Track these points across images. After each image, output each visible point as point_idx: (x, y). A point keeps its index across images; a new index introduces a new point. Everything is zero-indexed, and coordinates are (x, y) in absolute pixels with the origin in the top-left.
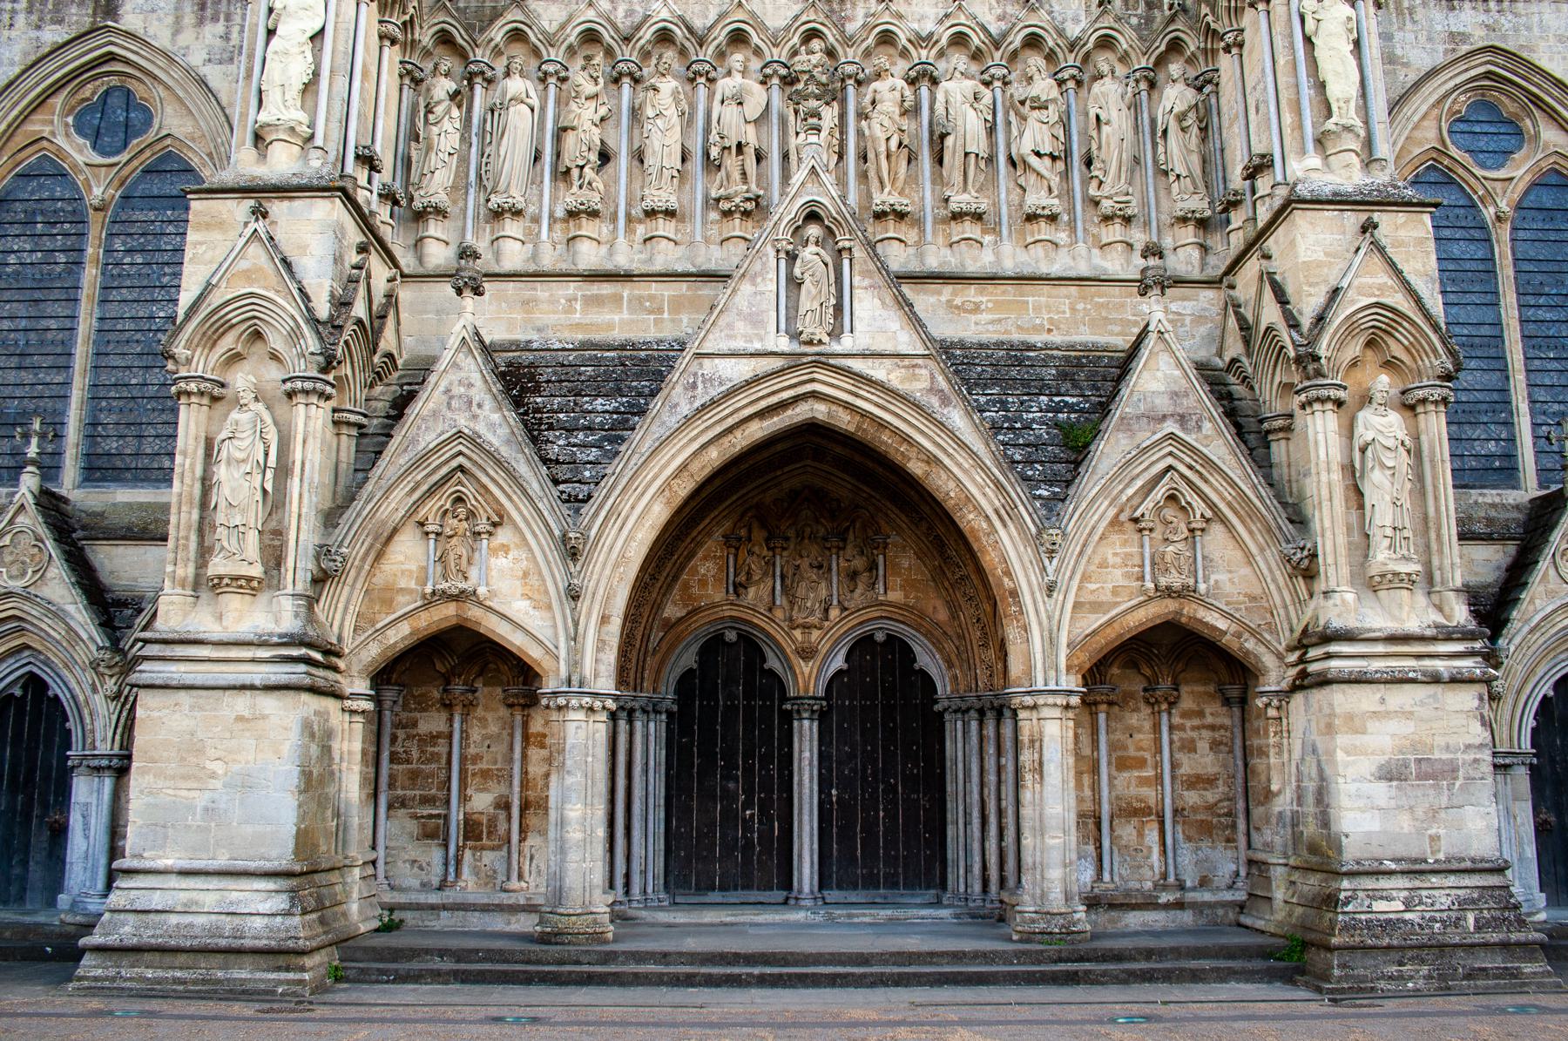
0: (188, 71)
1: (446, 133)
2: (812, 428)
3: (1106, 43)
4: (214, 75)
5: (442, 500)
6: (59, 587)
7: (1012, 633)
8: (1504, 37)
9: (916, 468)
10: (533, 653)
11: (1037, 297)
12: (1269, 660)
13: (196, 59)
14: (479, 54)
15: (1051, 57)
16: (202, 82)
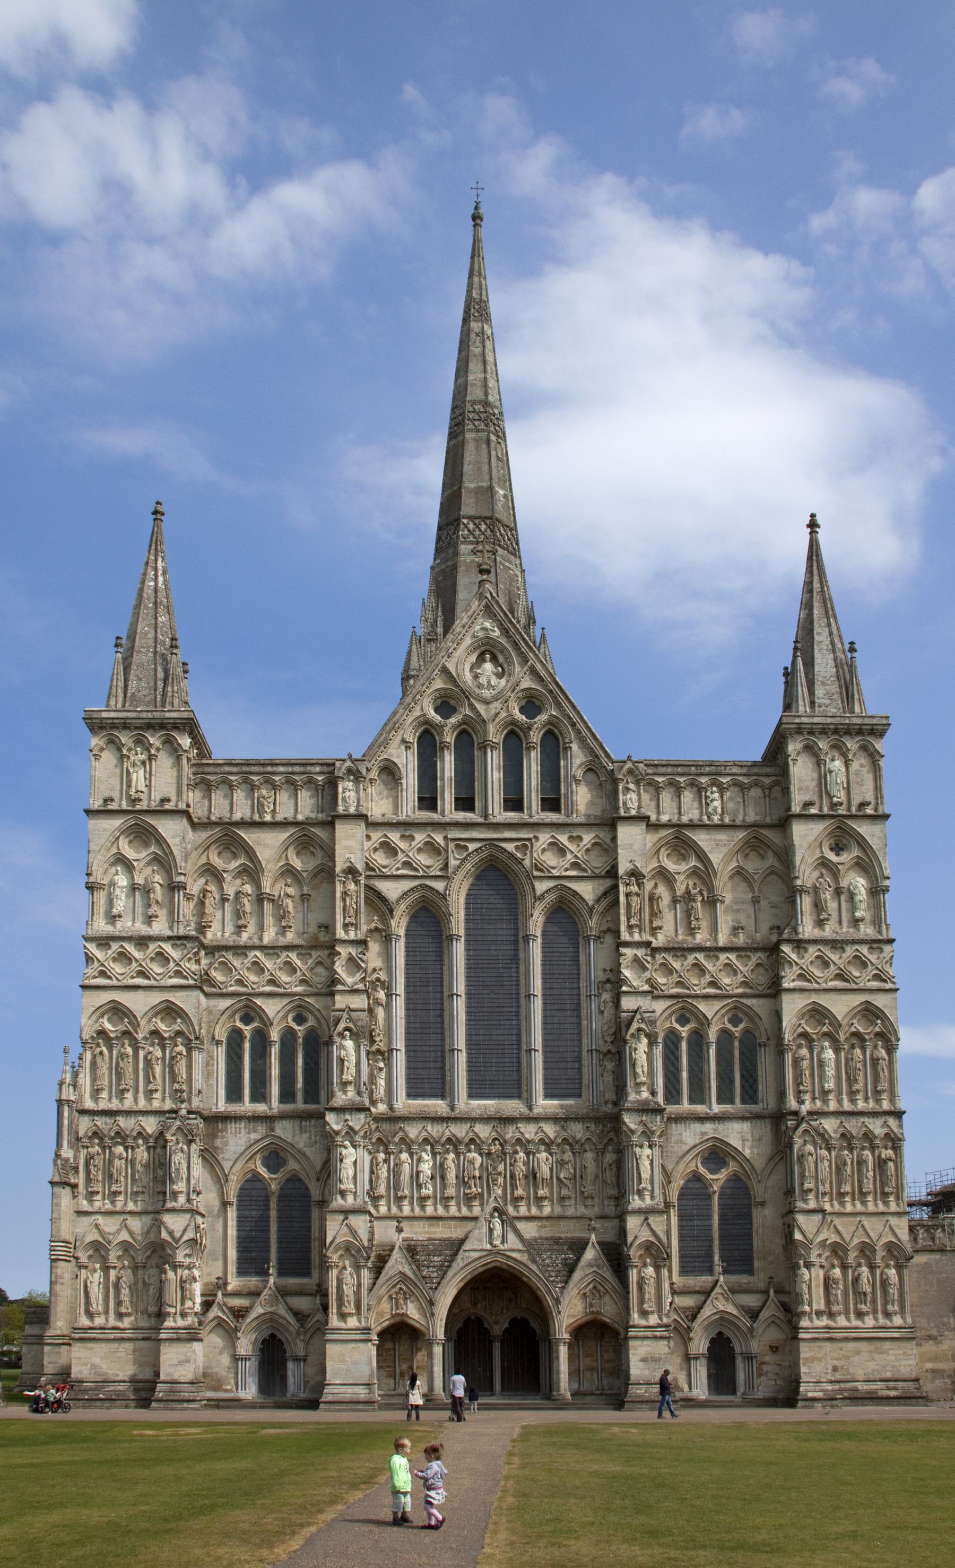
0: (299, 1151)
1: (383, 1172)
2: (496, 1267)
3: (588, 1139)
4: (308, 1151)
5: (396, 1289)
6: (282, 1311)
7: (551, 1323)
8: (719, 1133)
9: (525, 1279)
10: (423, 1329)
11: (562, 1223)
12: (621, 1330)
13: (301, 1145)
14: (392, 1146)
15: (571, 1145)
16: (304, 1154)
